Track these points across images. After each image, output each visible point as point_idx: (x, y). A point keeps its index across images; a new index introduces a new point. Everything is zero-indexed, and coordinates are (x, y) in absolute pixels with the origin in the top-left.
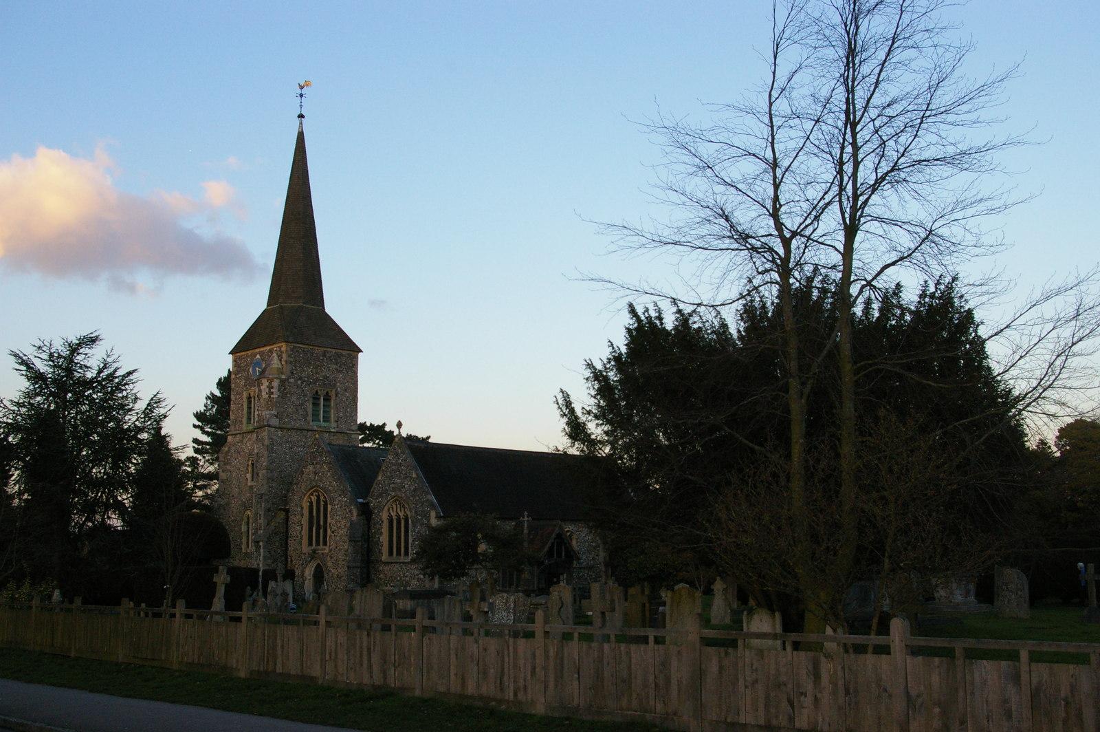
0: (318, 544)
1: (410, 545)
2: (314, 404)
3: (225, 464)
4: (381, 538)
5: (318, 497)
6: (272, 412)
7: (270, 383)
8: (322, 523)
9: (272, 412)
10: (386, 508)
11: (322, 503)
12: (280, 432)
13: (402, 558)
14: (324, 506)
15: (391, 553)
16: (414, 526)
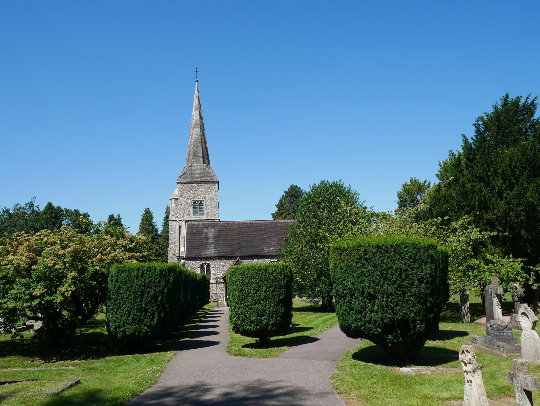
2: (194, 208)
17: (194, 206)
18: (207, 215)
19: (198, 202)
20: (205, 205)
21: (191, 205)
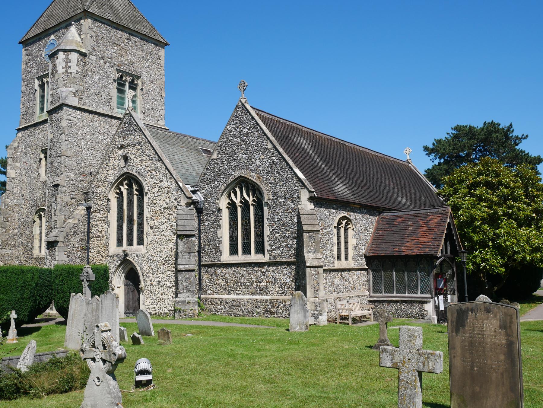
0: (130, 243)
1: (266, 239)
3: (14, 161)
4: (219, 232)
5: (130, 186)
6: (70, 89)
7: (68, 56)
8: (135, 217)
9: (70, 89)
12: (79, 113)
15: (234, 251)
17: (119, 84)
18: (144, 113)
19: (129, 79)
20: (142, 89)
21: (114, 81)
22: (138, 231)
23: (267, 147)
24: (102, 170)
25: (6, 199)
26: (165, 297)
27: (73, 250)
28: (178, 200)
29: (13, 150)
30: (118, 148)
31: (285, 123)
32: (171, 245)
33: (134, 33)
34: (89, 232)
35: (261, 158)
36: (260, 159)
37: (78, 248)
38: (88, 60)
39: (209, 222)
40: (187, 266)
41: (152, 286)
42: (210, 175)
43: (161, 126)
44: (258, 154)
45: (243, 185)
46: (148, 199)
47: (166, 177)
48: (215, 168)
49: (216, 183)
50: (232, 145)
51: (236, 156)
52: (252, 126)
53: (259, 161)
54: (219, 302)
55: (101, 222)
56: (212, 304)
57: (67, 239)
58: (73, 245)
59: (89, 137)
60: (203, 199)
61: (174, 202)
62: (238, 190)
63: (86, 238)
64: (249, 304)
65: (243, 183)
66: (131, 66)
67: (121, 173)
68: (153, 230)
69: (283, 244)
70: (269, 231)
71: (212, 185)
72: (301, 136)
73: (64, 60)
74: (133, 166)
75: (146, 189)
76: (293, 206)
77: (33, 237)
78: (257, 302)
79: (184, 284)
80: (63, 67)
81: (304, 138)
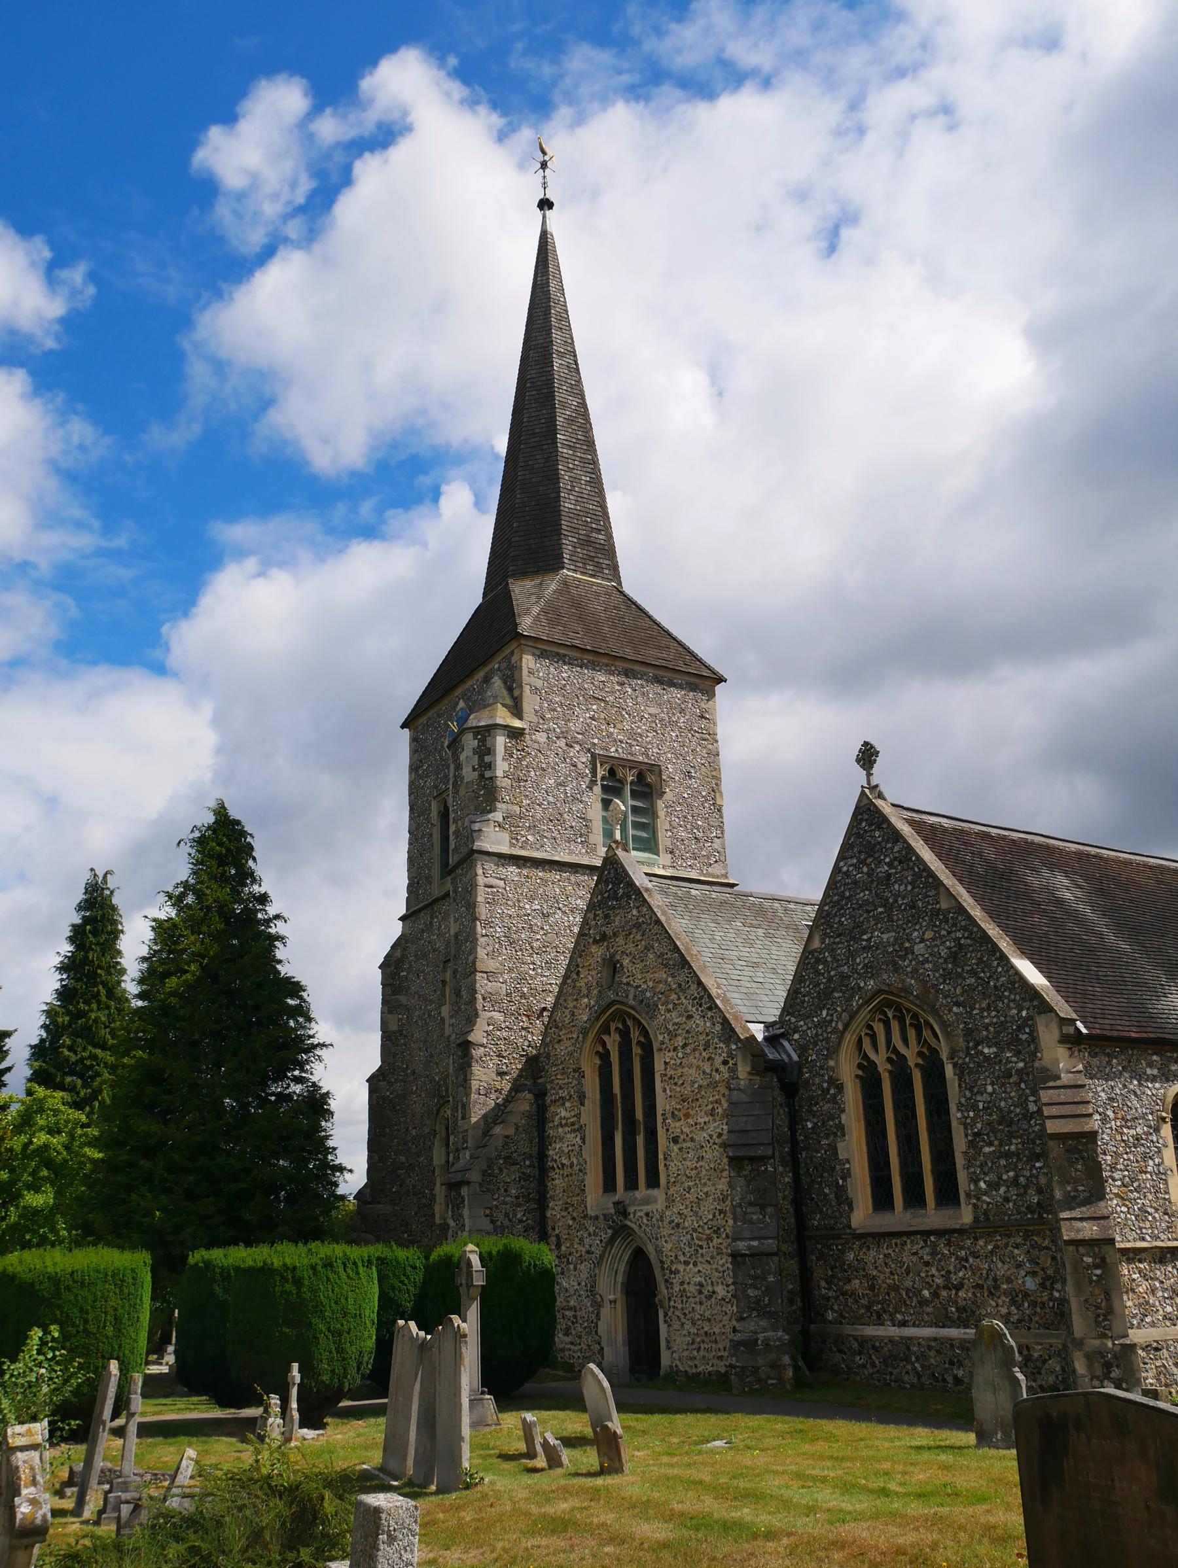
0: (632, 1185)
1: (960, 1161)
4: (841, 1146)
5: (625, 1034)
7: (483, 741)
8: (639, 1115)
10: (849, 1039)
11: (637, 1050)
13: (933, 1217)
14: (642, 1058)
15: (882, 1200)
16: (970, 1087)
22: (647, 1151)
23: (938, 906)
24: (565, 1001)
25: (381, 1083)
26: (716, 1330)
27: (504, 1203)
28: (730, 1065)
29: (392, 968)
30: (596, 942)
31: (1004, 838)
32: (722, 1185)
33: (637, 668)
34: (542, 1156)
35: (926, 937)
36: (923, 941)
37: (517, 1198)
38: (529, 743)
39: (815, 1120)
40: (755, 1243)
41: (685, 1299)
42: (809, 993)
43: (718, 877)
44: (917, 927)
45: (890, 1016)
46: (663, 1067)
47: (701, 1006)
48: (817, 973)
49: (824, 1013)
50: (854, 909)
51: (865, 937)
52: (897, 855)
53: (922, 945)
54: (855, 1346)
55: (567, 1129)
56: (840, 1351)
57: (490, 1175)
58: (506, 1190)
59: (538, 921)
60: (795, 1058)
61: (722, 1068)
62: (879, 1028)
63: (536, 1171)
64: (933, 1353)
65: (890, 1007)
66: (634, 743)
67: (603, 1003)
68: (678, 1146)
69: (1005, 1177)
70: (964, 1141)
71: (815, 1019)
72: (1052, 867)
73: (475, 751)
74: (628, 984)
75: (658, 1038)
76: (1021, 1065)
77: (433, 1172)
78: (952, 1345)
79: (751, 1292)
80: (473, 767)
81: (1065, 872)
